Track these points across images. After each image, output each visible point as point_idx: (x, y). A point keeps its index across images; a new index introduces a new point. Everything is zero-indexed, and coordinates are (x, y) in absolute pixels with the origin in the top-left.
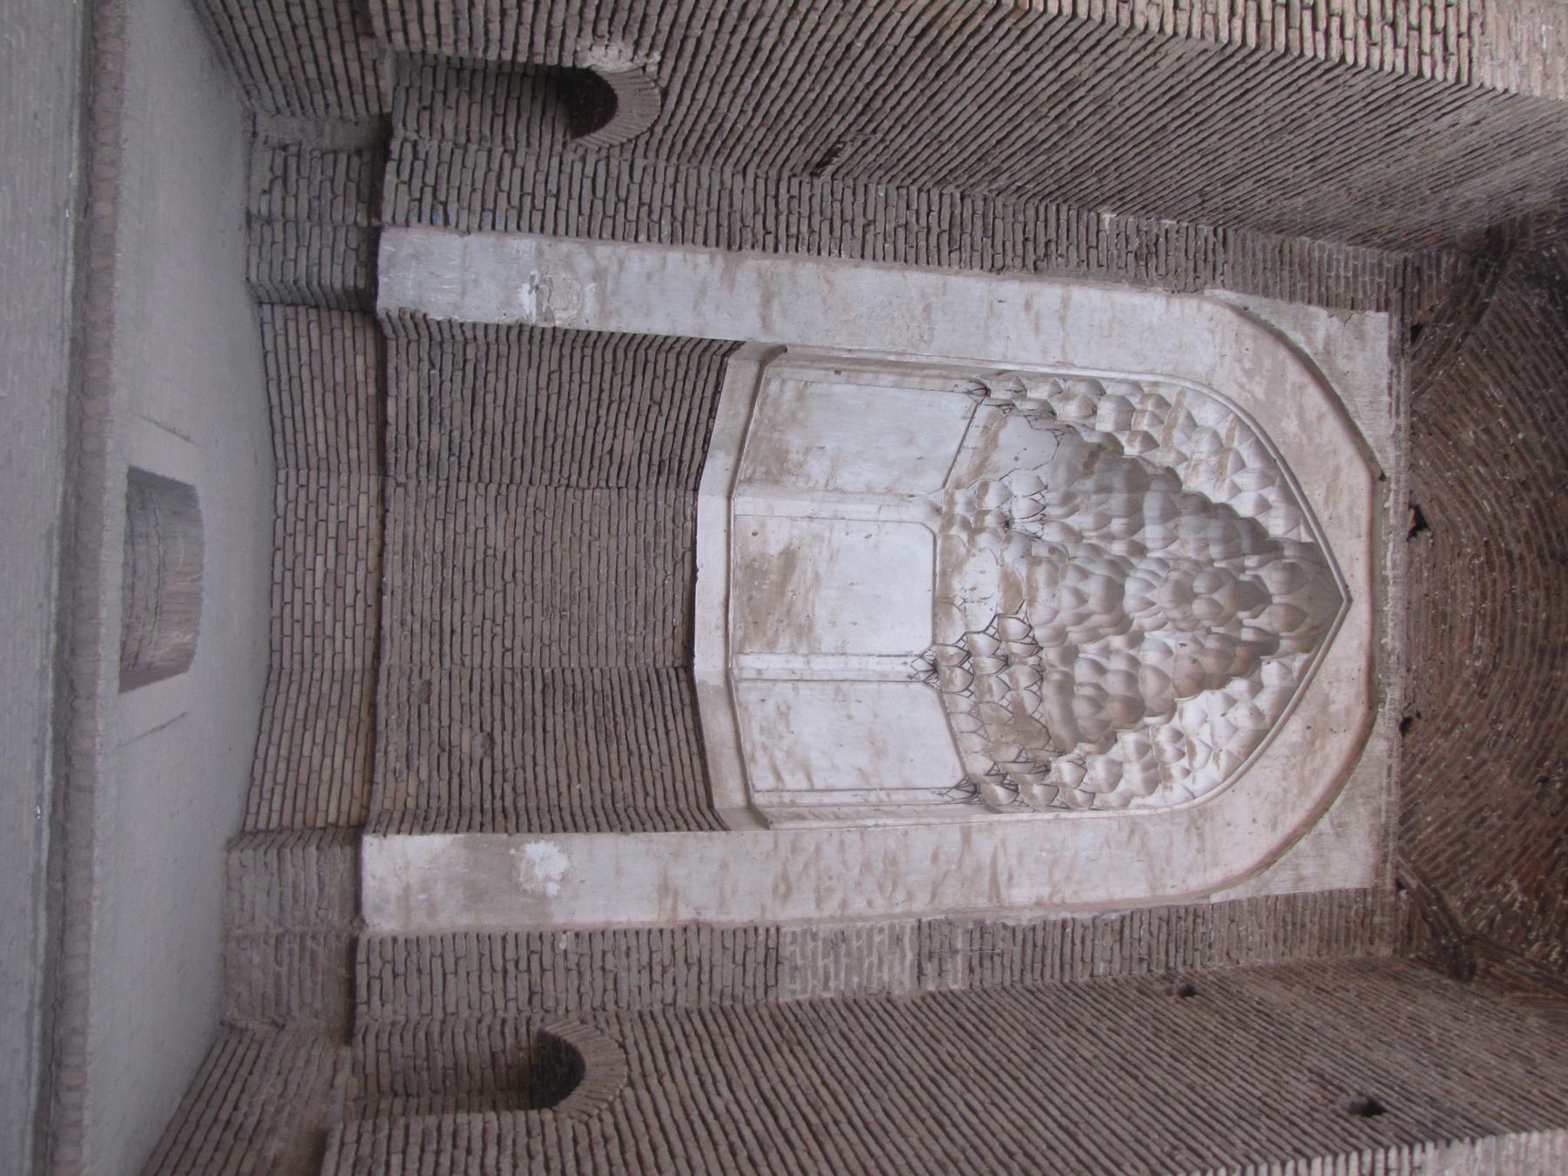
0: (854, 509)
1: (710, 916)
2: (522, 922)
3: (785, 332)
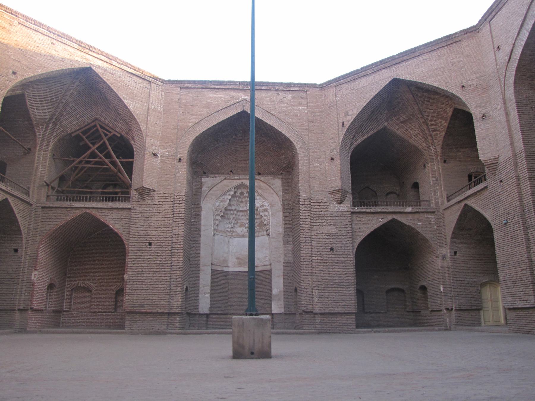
0: (230, 250)
1: (282, 271)
2: (283, 294)
3: (210, 263)
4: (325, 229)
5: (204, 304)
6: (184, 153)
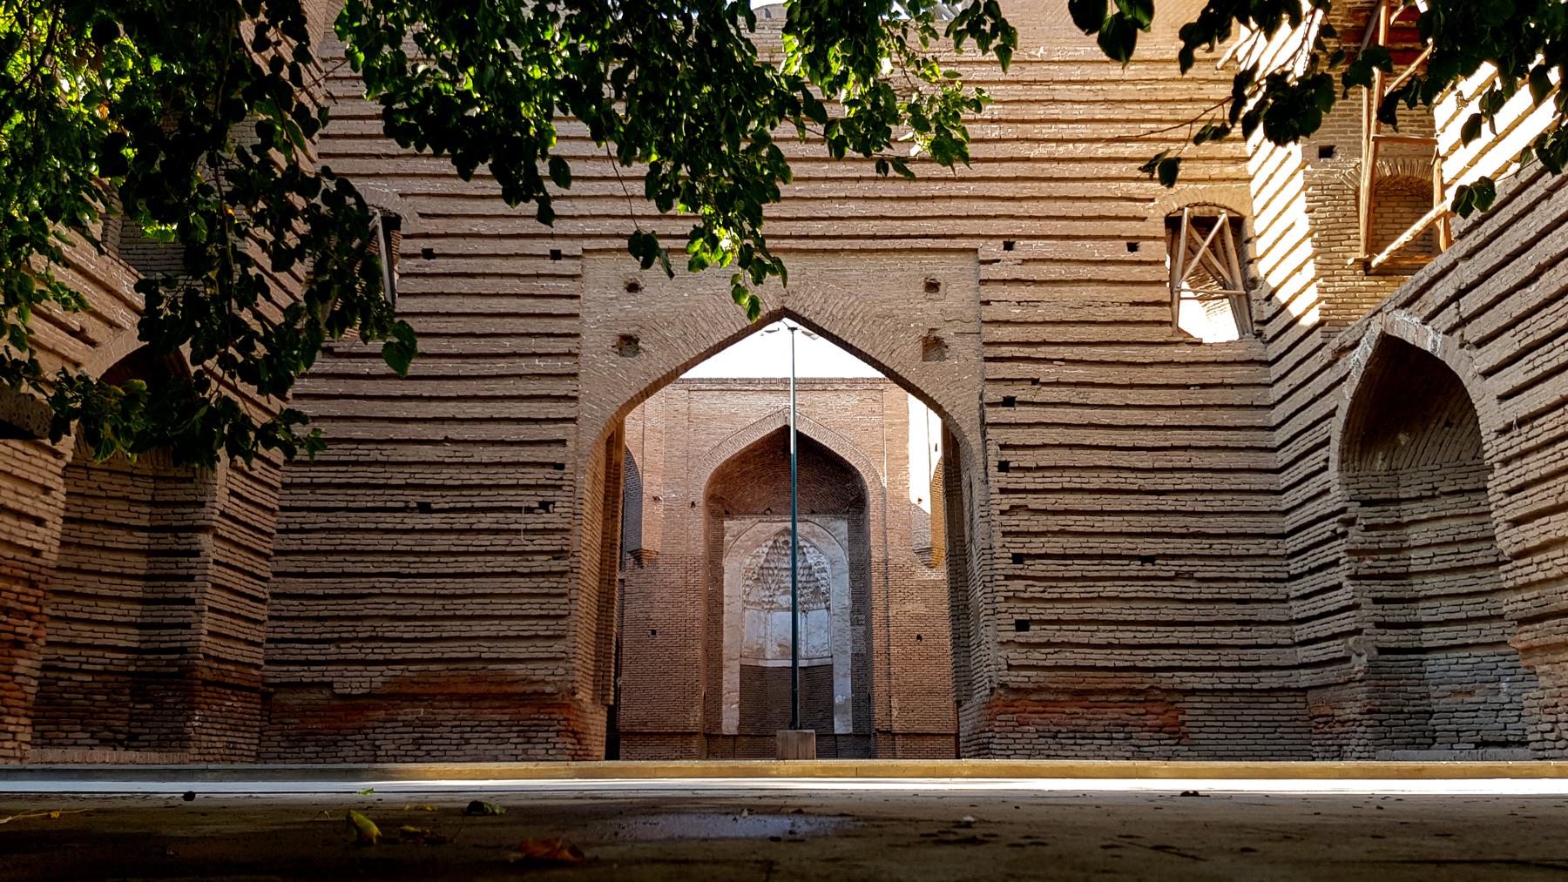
2: (850, 703)
4: (909, 607)
5: (730, 720)
6: (699, 496)
